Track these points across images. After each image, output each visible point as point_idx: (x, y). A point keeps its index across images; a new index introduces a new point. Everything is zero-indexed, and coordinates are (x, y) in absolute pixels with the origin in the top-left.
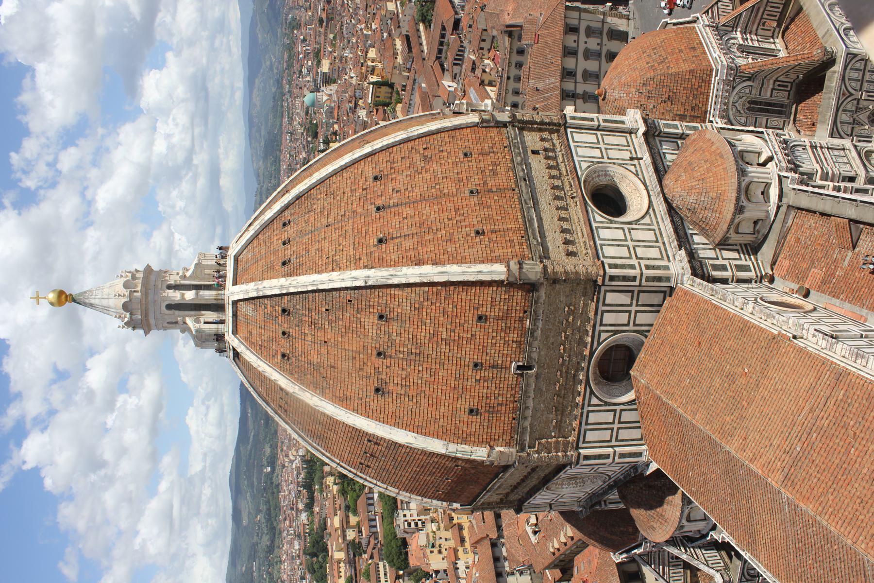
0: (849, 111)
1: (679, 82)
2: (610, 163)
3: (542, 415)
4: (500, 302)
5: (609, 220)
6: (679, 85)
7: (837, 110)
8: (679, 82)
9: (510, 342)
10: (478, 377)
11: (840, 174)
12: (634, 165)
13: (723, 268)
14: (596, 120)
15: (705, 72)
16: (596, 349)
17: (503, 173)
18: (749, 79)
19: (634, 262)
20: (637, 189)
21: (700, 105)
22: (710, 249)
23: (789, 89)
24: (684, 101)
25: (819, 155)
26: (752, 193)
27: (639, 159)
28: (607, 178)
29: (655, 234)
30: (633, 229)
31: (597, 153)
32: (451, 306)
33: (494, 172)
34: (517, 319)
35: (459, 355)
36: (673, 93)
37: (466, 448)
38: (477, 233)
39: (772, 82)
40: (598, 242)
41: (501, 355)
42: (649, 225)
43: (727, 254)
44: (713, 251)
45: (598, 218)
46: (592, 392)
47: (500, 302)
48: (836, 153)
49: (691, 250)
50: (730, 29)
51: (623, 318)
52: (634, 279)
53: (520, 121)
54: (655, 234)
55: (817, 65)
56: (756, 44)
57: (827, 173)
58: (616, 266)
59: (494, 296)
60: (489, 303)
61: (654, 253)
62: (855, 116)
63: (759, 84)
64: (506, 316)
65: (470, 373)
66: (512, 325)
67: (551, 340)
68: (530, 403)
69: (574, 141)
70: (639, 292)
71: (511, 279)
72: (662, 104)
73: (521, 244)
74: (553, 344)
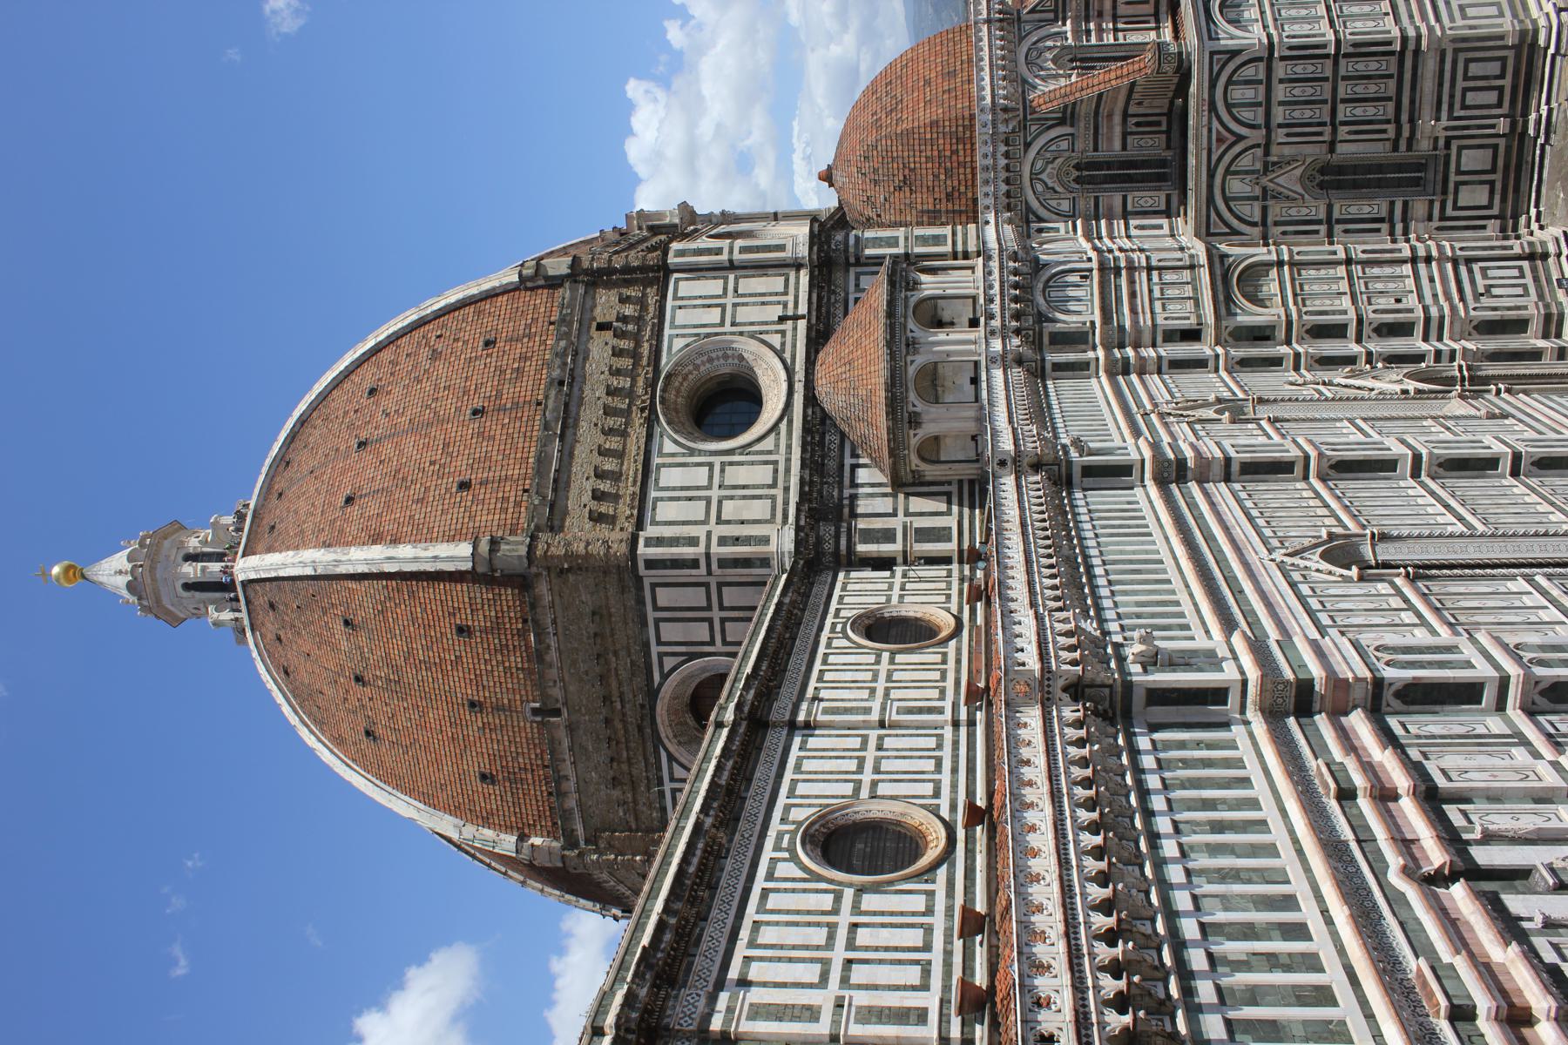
0: (1247, 172)
1: (917, 148)
2: (733, 334)
3: (598, 790)
4: (483, 605)
5: (688, 448)
6: (917, 154)
7: (1211, 175)
8: (917, 148)
9: (514, 670)
10: (480, 725)
11: (1154, 326)
12: (783, 333)
13: (888, 536)
14: (726, 251)
15: (960, 122)
16: (661, 685)
17: (532, 373)
18: (1061, 122)
19: (699, 532)
20: (776, 380)
21: (962, 189)
22: (885, 495)
23: (1164, 128)
24: (930, 184)
25: (1118, 288)
26: (948, 384)
27: (796, 318)
28: (730, 361)
29: (776, 471)
30: (731, 464)
31: (714, 316)
32: (419, 610)
33: (519, 371)
34: (515, 632)
35: (447, 688)
36: (910, 170)
37: (489, 833)
38: (464, 486)
39: (1117, 119)
40: (653, 494)
41: (504, 690)
42: (770, 452)
43: (917, 504)
44: (890, 499)
45: (669, 447)
46: (671, 758)
47: (483, 605)
48: (1169, 277)
49: (841, 498)
50: (1051, 16)
51: (701, 632)
52: (694, 564)
53: (588, 272)
54: (776, 471)
55: (1176, 80)
56: (1109, 39)
57: (1121, 328)
58: (659, 541)
59: (472, 595)
60: (467, 606)
61: (759, 509)
62: (1264, 181)
63: (1087, 129)
64: (497, 627)
65: (468, 717)
66: (510, 642)
67: (583, 667)
68: (568, 770)
69: (675, 298)
70: (720, 585)
71: (481, 569)
72: (897, 194)
73: (518, 504)
74: (587, 673)
